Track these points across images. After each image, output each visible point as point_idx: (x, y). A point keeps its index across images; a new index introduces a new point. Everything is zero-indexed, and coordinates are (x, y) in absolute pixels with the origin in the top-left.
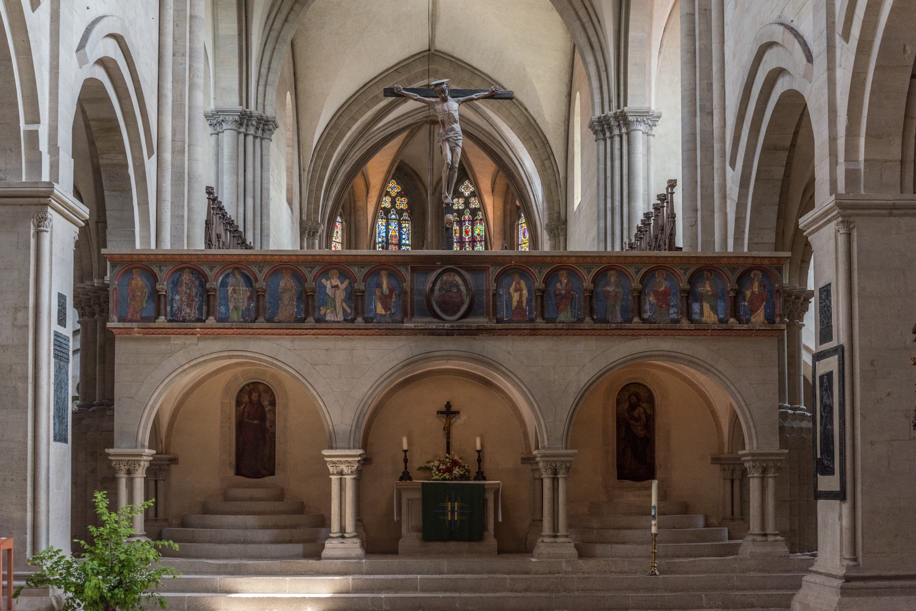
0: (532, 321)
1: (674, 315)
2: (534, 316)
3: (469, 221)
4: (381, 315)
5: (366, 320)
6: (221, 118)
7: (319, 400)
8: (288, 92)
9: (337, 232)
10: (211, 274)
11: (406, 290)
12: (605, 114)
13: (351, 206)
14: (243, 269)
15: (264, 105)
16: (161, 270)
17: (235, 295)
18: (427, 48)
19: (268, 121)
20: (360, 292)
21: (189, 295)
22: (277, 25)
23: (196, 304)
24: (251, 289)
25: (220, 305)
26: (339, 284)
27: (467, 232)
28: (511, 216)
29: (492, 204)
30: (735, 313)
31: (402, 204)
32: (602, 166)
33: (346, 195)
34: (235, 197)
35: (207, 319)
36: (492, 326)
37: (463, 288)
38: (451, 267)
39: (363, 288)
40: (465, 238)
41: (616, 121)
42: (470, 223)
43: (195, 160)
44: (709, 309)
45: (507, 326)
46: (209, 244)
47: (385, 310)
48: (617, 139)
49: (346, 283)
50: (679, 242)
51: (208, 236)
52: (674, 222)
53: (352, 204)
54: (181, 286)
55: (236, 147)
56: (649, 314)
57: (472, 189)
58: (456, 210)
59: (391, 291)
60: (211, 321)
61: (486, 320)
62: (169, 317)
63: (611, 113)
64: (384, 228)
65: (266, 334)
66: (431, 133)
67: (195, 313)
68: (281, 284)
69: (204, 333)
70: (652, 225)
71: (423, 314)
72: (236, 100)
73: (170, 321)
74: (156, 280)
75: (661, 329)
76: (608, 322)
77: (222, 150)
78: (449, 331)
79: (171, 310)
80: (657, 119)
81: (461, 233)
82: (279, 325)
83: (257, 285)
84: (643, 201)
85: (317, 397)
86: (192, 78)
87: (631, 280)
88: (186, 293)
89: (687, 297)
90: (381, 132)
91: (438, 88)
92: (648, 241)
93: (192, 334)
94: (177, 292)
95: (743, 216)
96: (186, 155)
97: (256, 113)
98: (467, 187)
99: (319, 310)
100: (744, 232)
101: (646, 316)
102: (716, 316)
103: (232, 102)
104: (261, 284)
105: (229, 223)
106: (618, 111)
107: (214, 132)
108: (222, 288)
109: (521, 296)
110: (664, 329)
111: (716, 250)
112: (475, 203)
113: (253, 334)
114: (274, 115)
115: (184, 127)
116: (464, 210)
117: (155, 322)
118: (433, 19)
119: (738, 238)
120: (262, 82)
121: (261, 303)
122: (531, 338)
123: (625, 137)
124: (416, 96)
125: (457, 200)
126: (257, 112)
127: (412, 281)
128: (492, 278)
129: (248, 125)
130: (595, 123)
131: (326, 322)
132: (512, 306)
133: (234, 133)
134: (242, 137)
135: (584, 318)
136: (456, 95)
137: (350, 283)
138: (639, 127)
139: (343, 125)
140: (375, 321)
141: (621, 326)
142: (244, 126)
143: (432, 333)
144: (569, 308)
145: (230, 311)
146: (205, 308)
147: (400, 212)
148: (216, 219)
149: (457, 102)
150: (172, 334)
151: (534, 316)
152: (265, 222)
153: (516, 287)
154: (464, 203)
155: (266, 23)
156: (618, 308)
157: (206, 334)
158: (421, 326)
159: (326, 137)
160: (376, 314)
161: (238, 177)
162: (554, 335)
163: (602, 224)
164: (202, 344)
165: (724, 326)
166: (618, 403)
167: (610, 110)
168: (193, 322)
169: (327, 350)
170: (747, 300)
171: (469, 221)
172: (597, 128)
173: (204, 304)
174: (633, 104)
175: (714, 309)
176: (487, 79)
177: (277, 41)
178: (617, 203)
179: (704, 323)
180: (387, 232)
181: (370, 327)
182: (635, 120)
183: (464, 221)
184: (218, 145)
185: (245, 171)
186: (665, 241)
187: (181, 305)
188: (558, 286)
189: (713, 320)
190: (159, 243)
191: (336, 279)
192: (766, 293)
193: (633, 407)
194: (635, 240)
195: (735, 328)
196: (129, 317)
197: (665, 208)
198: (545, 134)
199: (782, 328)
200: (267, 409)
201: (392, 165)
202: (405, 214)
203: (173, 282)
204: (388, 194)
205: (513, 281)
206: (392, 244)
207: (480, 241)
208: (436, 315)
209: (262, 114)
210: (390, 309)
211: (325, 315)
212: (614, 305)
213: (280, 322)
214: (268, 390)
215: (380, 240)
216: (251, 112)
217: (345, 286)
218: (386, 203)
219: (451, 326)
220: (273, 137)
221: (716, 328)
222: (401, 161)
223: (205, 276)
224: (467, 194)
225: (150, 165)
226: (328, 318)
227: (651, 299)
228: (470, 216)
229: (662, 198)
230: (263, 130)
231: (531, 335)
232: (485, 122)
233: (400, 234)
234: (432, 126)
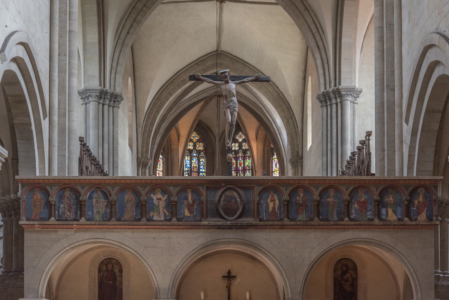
0: (281, 220)
1: (370, 216)
2: (282, 217)
3: (242, 157)
4: (187, 217)
5: (178, 220)
6: (88, 94)
7: (149, 269)
8: (130, 78)
9: (160, 165)
10: (82, 191)
11: (203, 201)
12: (327, 90)
13: (168, 148)
14: (102, 188)
15: (115, 86)
16: (52, 189)
17: (97, 204)
18: (215, 49)
19: (117, 96)
20: (174, 202)
21: (69, 204)
22: (123, 36)
23: (73, 210)
24: (107, 200)
25: (88, 210)
26: (162, 197)
27: (240, 164)
29: (256, 147)
30: (408, 214)
31: (200, 147)
32: (325, 123)
33: (165, 141)
34: (97, 143)
35: (80, 219)
36: (257, 223)
37: (238, 200)
38: (231, 186)
39: (176, 200)
40: (239, 168)
41: (334, 94)
42: (242, 158)
43: (72, 121)
44: (391, 212)
45: (266, 223)
46: (81, 173)
47: (190, 214)
48: (334, 106)
49: (166, 196)
50: (373, 171)
51: (81, 167)
52: (370, 158)
53: (169, 147)
54: (64, 199)
55: (97, 112)
56: (354, 215)
57: (244, 137)
58: (234, 150)
59: (194, 202)
60: (83, 220)
61: (253, 219)
62: (57, 218)
63: (330, 90)
64: (189, 162)
65: (117, 228)
66: (218, 103)
67: (73, 215)
68: (126, 197)
69: (79, 227)
70: (356, 159)
71: (213, 216)
72: (97, 83)
73: (58, 220)
74: (49, 195)
75: (362, 225)
76: (328, 220)
77: (89, 114)
78: (230, 226)
79: (58, 213)
80: (360, 93)
81: (237, 165)
82: (125, 223)
83: (111, 198)
84: (351, 144)
85: (148, 267)
86: (70, 70)
87: (343, 194)
88: (67, 203)
89: (378, 205)
90: (187, 102)
91: (223, 75)
92: (353, 169)
93: (71, 228)
94: (62, 203)
95: (413, 154)
96: (67, 117)
97: (110, 91)
98: (241, 136)
99: (149, 214)
100: (414, 164)
101: (352, 217)
102: (396, 217)
103: (95, 84)
104: (113, 197)
105: (93, 160)
106: (335, 88)
107: (83, 103)
108: (89, 200)
109: (274, 204)
110: (364, 225)
111: (397, 175)
112: (245, 146)
113: (108, 228)
114: (121, 92)
115: (66, 100)
116: (238, 150)
117: (48, 221)
118: (219, 30)
119: (410, 168)
120: (113, 72)
121: (113, 209)
122: (281, 230)
123: (339, 105)
124: (210, 80)
125: (234, 144)
126: (110, 90)
127: (207, 196)
128: (256, 193)
129: (105, 99)
130: (320, 96)
131: (154, 221)
132: (269, 211)
133: (97, 103)
134: (101, 106)
135: (314, 218)
136: (234, 79)
137: (168, 197)
138: (348, 98)
139: (163, 98)
140: (184, 220)
141: (337, 223)
142: (102, 99)
143: (219, 227)
144: (304, 211)
145: (95, 214)
146: (79, 212)
147: (199, 152)
148: (85, 157)
149: (235, 84)
150: (59, 228)
151: (282, 217)
152: (115, 159)
153: (271, 199)
154: (239, 146)
155: (116, 35)
156: (335, 212)
157: (80, 228)
158: (212, 223)
159: (153, 106)
160: (184, 216)
161: (99, 131)
162: (295, 229)
163: (325, 159)
164: (77, 235)
165: (401, 223)
166: (335, 270)
167: (330, 88)
168: (71, 221)
169: (154, 238)
170: (415, 206)
171: (242, 157)
172: (322, 99)
173: (78, 210)
174: (345, 84)
175: (395, 212)
176: (253, 68)
177: (122, 46)
178: (334, 146)
179: (389, 221)
180: (191, 164)
181: (181, 224)
182: (346, 94)
183: (239, 157)
184: (86, 111)
185: (103, 127)
186: (364, 170)
187: (64, 210)
188: (298, 198)
189: (394, 219)
190: (50, 172)
191: (159, 194)
192: (427, 202)
193: (344, 273)
194: (346, 169)
195: (408, 224)
196: (33, 218)
197: (364, 149)
198: (289, 103)
199: (437, 224)
200: (117, 274)
201: (194, 122)
202: (202, 153)
203: (59, 196)
204: (191, 140)
205: (270, 195)
206: (194, 172)
207: (249, 170)
208: (221, 217)
209: (113, 91)
210: (193, 213)
211: (153, 216)
212: (333, 209)
213: (125, 221)
214: (118, 263)
215: (186, 169)
216: (107, 90)
217: (165, 199)
218: (190, 147)
219: (231, 223)
220: (120, 106)
221: (396, 224)
222: (200, 120)
223: (79, 193)
224: (240, 141)
225: (45, 124)
226: (155, 218)
227: (355, 206)
228: (243, 154)
229: (363, 143)
230: (114, 102)
231: (281, 229)
232: (252, 95)
233: (199, 166)
234: (219, 98)
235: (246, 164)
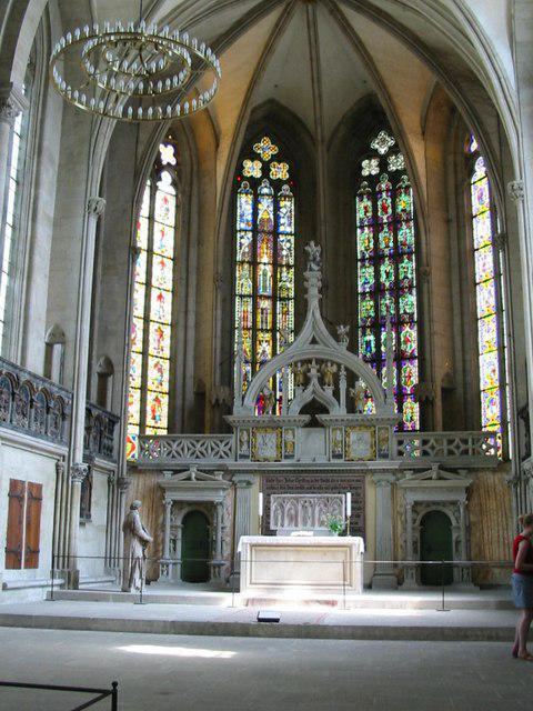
3: (388, 190)
13: (192, 169)
27: (385, 209)
28: (456, 172)
31: (280, 172)
57: (391, 142)
98: (383, 141)
116: (378, 176)
125: (367, 161)
154: (379, 165)
171: (388, 190)
183: (380, 192)
202: (286, 187)
207: (407, 221)
215: (243, 226)
218: (253, 169)
233: (277, 217)
235: (400, 208)
